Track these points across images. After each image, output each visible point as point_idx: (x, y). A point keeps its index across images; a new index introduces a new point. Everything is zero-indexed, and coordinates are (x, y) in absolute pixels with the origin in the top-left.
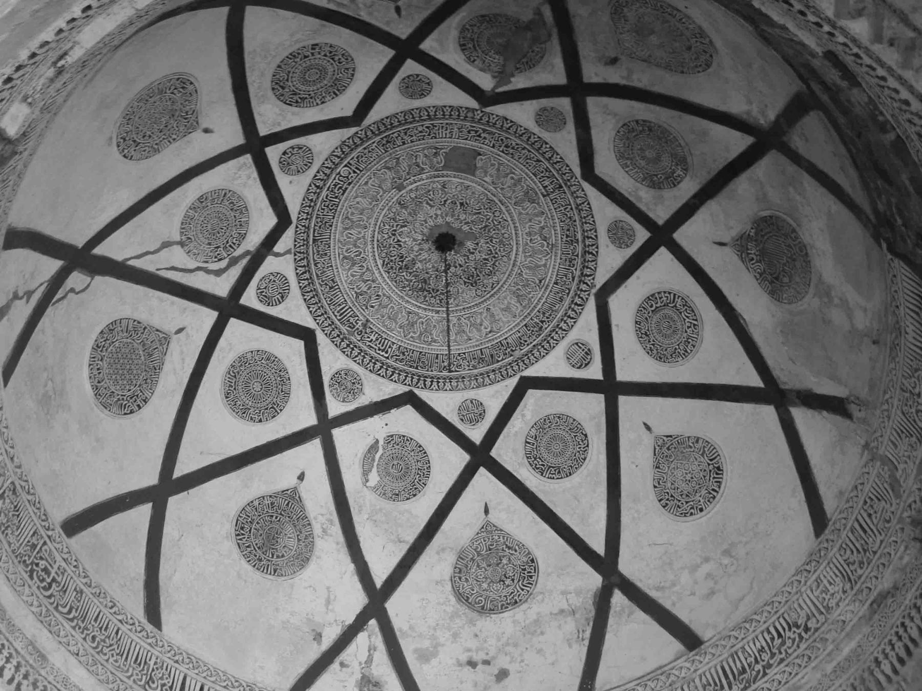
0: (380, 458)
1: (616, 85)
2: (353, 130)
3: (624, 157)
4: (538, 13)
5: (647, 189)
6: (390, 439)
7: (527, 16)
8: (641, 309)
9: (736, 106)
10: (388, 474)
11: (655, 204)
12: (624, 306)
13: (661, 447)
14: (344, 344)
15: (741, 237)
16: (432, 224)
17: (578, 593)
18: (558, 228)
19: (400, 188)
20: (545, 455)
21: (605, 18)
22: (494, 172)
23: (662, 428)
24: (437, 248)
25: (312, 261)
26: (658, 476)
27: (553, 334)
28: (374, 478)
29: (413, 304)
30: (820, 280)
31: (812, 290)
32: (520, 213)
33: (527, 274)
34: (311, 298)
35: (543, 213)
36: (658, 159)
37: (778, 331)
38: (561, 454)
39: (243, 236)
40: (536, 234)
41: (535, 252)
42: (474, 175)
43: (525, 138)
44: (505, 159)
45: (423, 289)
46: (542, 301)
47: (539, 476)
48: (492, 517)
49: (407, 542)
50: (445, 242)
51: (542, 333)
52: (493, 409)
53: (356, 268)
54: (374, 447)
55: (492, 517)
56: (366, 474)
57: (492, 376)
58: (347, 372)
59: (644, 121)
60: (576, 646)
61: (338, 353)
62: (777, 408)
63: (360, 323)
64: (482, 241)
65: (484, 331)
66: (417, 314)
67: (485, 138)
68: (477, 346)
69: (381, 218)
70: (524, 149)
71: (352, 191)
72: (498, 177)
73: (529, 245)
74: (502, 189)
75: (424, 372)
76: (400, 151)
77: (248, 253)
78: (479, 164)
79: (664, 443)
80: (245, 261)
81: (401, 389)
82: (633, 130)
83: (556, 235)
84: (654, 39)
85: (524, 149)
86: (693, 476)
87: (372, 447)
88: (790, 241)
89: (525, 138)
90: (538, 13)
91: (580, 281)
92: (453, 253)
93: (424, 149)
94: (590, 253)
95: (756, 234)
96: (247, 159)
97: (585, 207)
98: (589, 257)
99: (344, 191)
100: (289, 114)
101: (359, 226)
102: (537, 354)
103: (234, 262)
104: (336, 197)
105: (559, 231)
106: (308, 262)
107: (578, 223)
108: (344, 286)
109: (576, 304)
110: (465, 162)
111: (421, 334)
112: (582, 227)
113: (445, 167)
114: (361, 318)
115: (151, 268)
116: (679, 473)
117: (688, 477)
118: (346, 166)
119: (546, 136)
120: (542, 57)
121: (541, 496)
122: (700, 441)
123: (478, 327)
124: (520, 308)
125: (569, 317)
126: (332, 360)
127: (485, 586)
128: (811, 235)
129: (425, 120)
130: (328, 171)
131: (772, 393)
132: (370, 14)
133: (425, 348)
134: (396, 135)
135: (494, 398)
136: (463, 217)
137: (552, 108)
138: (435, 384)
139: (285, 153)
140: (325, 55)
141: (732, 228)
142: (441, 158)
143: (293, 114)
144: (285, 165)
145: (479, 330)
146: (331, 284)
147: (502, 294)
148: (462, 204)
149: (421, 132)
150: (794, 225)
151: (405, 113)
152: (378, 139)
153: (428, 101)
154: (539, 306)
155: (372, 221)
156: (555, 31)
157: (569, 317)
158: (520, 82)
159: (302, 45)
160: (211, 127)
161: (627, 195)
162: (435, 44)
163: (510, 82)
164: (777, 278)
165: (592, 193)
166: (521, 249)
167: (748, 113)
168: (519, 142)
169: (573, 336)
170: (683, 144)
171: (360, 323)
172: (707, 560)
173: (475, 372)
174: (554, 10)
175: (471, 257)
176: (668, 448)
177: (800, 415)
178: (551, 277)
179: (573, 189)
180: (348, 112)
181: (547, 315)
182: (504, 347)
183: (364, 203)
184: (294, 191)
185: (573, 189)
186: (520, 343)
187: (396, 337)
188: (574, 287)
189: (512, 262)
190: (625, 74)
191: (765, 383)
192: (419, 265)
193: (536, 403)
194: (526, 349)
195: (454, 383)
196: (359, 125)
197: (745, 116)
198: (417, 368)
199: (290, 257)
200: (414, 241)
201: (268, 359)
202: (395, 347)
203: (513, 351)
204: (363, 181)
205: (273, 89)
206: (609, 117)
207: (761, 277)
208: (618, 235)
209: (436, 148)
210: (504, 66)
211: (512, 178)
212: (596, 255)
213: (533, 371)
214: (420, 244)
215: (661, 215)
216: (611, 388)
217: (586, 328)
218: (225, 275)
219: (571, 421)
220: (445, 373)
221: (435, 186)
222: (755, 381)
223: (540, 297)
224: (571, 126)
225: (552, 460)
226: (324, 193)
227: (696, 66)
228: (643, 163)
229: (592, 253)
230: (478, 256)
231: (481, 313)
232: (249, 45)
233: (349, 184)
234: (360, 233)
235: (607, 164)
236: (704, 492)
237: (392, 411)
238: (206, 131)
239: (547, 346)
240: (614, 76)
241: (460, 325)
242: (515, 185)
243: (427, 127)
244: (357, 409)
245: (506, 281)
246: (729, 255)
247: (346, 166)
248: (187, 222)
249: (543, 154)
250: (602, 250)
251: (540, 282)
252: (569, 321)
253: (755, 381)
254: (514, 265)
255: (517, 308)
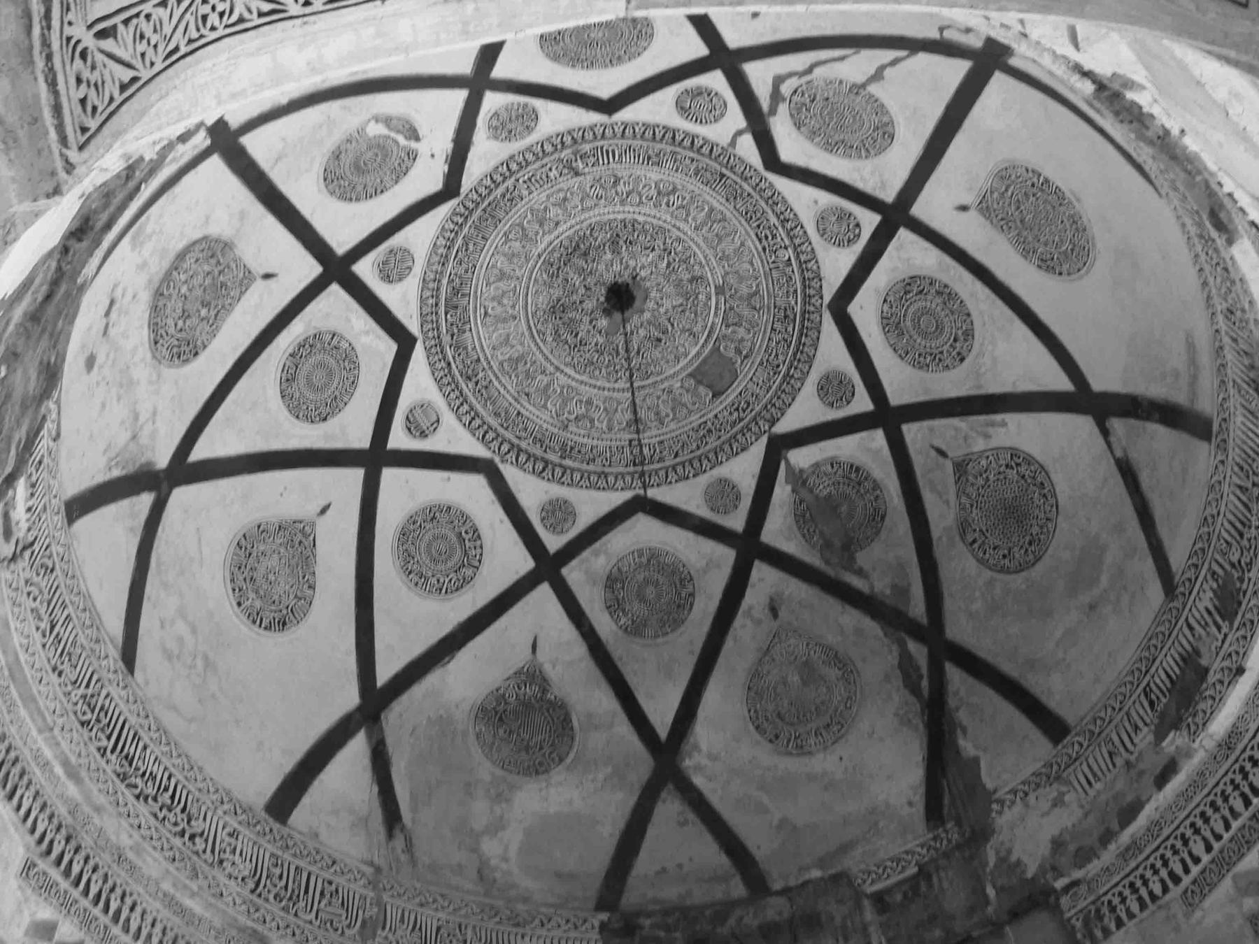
0: (396, 142)
1: (741, 595)
2: (827, 298)
3: (652, 559)
4: (860, 573)
5: (609, 568)
6: (413, 156)
7: (862, 559)
8: (465, 518)
9: (703, 733)
10: (370, 148)
11: (586, 572)
12: (469, 493)
13: (302, 531)
14: (568, 140)
15: (545, 680)
16: (653, 294)
17: (153, 435)
18: (585, 440)
19: (720, 290)
20: (312, 360)
21: (831, 639)
22: (687, 398)
23: (323, 528)
24: (616, 283)
25: (699, 157)
26: (272, 529)
27: (457, 393)
28: (375, 130)
29: (565, 231)
30: (513, 788)
31: (499, 772)
32: (619, 403)
33: (542, 380)
34: (652, 132)
35: (610, 429)
36: (642, 599)
37: (442, 712)
38: (309, 383)
39: (798, 125)
40: (587, 411)
41: (565, 403)
42: (690, 375)
43: (711, 455)
44: (695, 419)
45: (580, 249)
46: (502, 391)
47: (290, 351)
48: (259, 284)
49: (272, 168)
50: (621, 297)
51: (460, 377)
52: (388, 294)
53: (653, 192)
54: (414, 135)
55: (259, 284)
56: (387, 121)
57: (431, 301)
58: (529, 130)
59: (692, 605)
60: (102, 461)
61: (561, 128)
62: (359, 709)
63: (581, 166)
64: (601, 340)
65: (490, 305)
66: (550, 232)
67: (731, 413)
68: (476, 292)
69: (694, 247)
70: (698, 448)
71: (752, 244)
72: (674, 400)
73: (578, 394)
74: (658, 398)
75: (475, 216)
76: (765, 318)
77: (773, 111)
78: (702, 389)
79: (306, 536)
80: (765, 105)
81: (468, 182)
82: (684, 586)
83: (576, 435)
84: (795, 679)
85: (698, 448)
86: (269, 578)
87: (415, 131)
88: (547, 750)
89: (711, 455)
90: (860, 573)
91: (513, 445)
92: (602, 299)
93: (753, 344)
94: (543, 469)
95: (549, 702)
96: (889, 196)
97: (602, 483)
98: (540, 466)
99: (760, 240)
100: (900, 265)
101: (704, 224)
102: (439, 366)
103: (776, 96)
104: (759, 226)
105: (581, 440)
106: (703, 155)
107: (584, 467)
108: (640, 171)
109: (486, 432)
110: (712, 375)
111: (523, 229)
112: (579, 470)
113: (716, 349)
114: (586, 170)
115: (866, 54)
116: (273, 562)
117: (271, 577)
118: (789, 259)
119: (704, 479)
120: (804, 536)
121: (264, 355)
122: (311, 592)
123: (498, 299)
124: (500, 358)
125: (473, 419)
126: (556, 118)
127: (184, 290)
128: (560, 784)
129: (789, 369)
130: (797, 241)
131: (375, 701)
132: (956, 429)
133: (503, 228)
134: (790, 329)
135: (402, 298)
136: (642, 332)
137: (736, 507)
138: (452, 226)
139: (858, 225)
140: (941, 353)
141: (554, 667)
142: (731, 354)
143: (894, 269)
144: (843, 216)
145: (493, 299)
146: (655, 159)
147: (528, 340)
148: (659, 340)
149: (777, 355)
150: (568, 760)
151: (810, 361)
152: (798, 309)
153: (809, 388)
154: (496, 383)
155: (700, 241)
156: (831, 572)
157: (473, 419)
158: (782, 492)
159: (974, 352)
160: (964, 215)
161: (605, 539)
162: (874, 445)
163: (787, 482)
164: (501, 719)
165: (617, 498)
166: (574, 384)
167: (696, 747)
168: (708, 448)
169: (448, 418)
170: (660, 640)
171: (581, 166)
172: (194, 631)
173: (445, 281)
174: (859, 593)
175: (586, 319)
176: (297, 539)
177: (358, 746)
178: (529, 410)
179: (628, 479)
180: (853, 309)
181: (483, 391)
182: (460, 327)
183: (728, 247)
184: (806, 201)
185: (628, 479)
186: (458, 347)
187: (539, 197)
188: (508, 435)
189: (562, 367)
190: (757, 613)
191: (383, 688)
192: (609, 256)
193: (377, 350)
194: (449, 353)
195: (441, 251)
196: (830, 306)
197: (692, 740)
198: (484, 210)
199: (724, 140)
200: (642, 264)
201: (619, 58)
202: (525, 193)
203: (452, 336)
204: (757, 262)
205: (946, 286)
206: (704, 563)
207: (499, 696)
208: (558, 512)
209: (746, 357)
210: (811, 491)
211: (667, 415)
212: (540, 474)
213: (419, 354)
214: (635, 269)
215: (573, 573)
216: (375, 458)
217: (453, 437)
218: (770, 82)
219: (345, 399)
220: (460, 241)
221: (699, 325)
222: (384, 673)
223: (506, 388)
224: (703, 512)
225: (305, 368)
226: (773, 220)
227: (756, 711)
228: (640, 577)
229: (544, 469)
230: (584, 328)
231: (513, 307)
232: (1021, 330)
233: (764, 249)
234: (694, 219)
235: (644, 532)
236: (258, 604)
237: (446, 168)
238: (964, 208)
239: (445, 381)
240: (754, 598)
241: (510, 278)
242: (657, 414)
243: (778, 366)
244: (474, 125)
245: (542, 352)
246: (521, 657)
247: (789, 259)
248: (881, 109)
249: (683, 464)
250: (544, 485)
251: (527, 395)
252: (469, 418)
253: (384, 673)
254: (557, 368)
255: (504, 354)
